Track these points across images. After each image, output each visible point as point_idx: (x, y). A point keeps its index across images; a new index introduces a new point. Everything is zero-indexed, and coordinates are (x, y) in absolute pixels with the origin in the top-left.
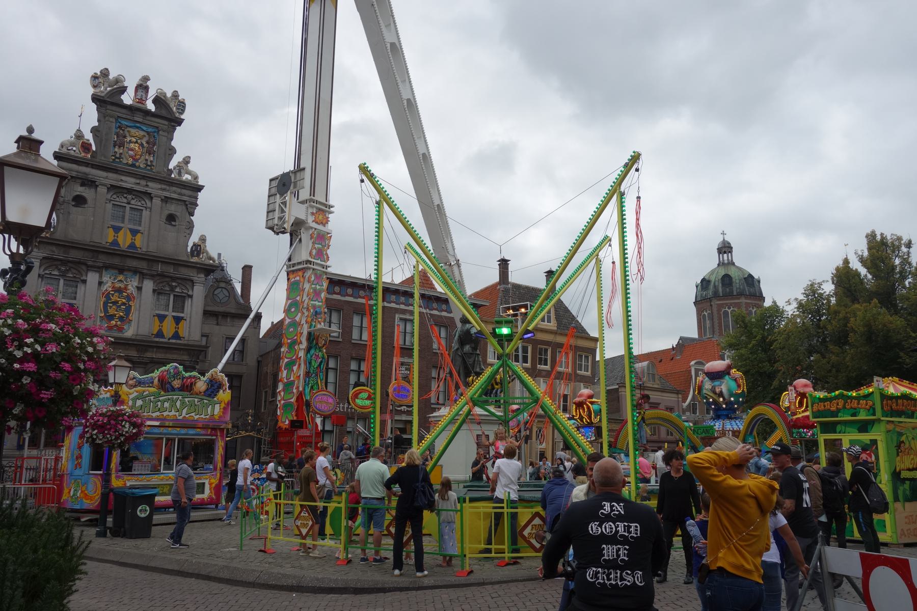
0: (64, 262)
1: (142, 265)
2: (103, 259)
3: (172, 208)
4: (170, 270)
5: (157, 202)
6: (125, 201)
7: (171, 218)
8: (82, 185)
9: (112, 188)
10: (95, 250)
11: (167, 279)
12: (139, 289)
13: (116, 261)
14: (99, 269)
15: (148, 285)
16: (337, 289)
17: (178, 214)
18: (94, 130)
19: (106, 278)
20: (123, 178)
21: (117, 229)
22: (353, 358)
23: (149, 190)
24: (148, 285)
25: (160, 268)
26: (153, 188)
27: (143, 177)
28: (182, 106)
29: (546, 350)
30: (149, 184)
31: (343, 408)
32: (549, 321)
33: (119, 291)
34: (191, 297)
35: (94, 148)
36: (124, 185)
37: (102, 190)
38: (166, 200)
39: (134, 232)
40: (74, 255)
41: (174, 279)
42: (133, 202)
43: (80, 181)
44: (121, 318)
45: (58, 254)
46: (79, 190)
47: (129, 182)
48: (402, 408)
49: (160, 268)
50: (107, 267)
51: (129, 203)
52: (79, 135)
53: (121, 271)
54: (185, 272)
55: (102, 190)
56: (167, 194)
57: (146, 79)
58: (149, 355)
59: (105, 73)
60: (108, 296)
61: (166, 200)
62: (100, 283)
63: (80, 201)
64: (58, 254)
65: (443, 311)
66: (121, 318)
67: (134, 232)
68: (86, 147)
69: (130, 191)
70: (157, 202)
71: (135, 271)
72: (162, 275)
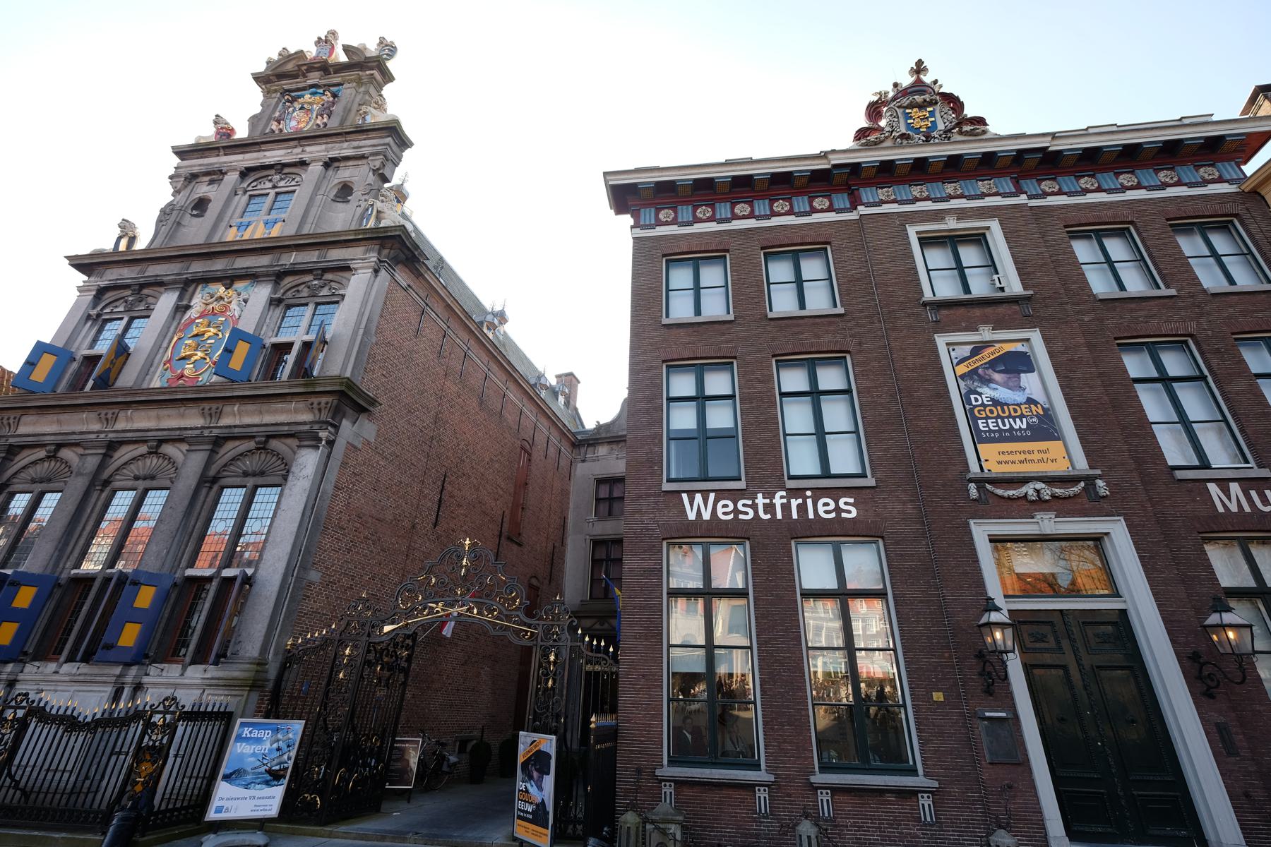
2: (198, 267)
3: (345, 174)
4: (312, 257)
5: (316, 168)
6: (269, 185)
8: (211, 182)
9: (245, 173)
11: (308, 278)
12: (246, 301)
13: (218, 265)
20: (267, 154)
23: (305, 157)
25: (291, 259)
26: (316, 151)
30: (308, 149)
31: (769, 508)
34: (343, 296)
36: (267, 161)
38: (330, 164)
42: (282, 183)
43: (207, 178)
46: (203, 189)
48: (1029, 489)
51: (274, 187)
53: (229, 280)
54: (336, 254)
69: (280, 167)
70: (316, 168)
72: (294, 272)
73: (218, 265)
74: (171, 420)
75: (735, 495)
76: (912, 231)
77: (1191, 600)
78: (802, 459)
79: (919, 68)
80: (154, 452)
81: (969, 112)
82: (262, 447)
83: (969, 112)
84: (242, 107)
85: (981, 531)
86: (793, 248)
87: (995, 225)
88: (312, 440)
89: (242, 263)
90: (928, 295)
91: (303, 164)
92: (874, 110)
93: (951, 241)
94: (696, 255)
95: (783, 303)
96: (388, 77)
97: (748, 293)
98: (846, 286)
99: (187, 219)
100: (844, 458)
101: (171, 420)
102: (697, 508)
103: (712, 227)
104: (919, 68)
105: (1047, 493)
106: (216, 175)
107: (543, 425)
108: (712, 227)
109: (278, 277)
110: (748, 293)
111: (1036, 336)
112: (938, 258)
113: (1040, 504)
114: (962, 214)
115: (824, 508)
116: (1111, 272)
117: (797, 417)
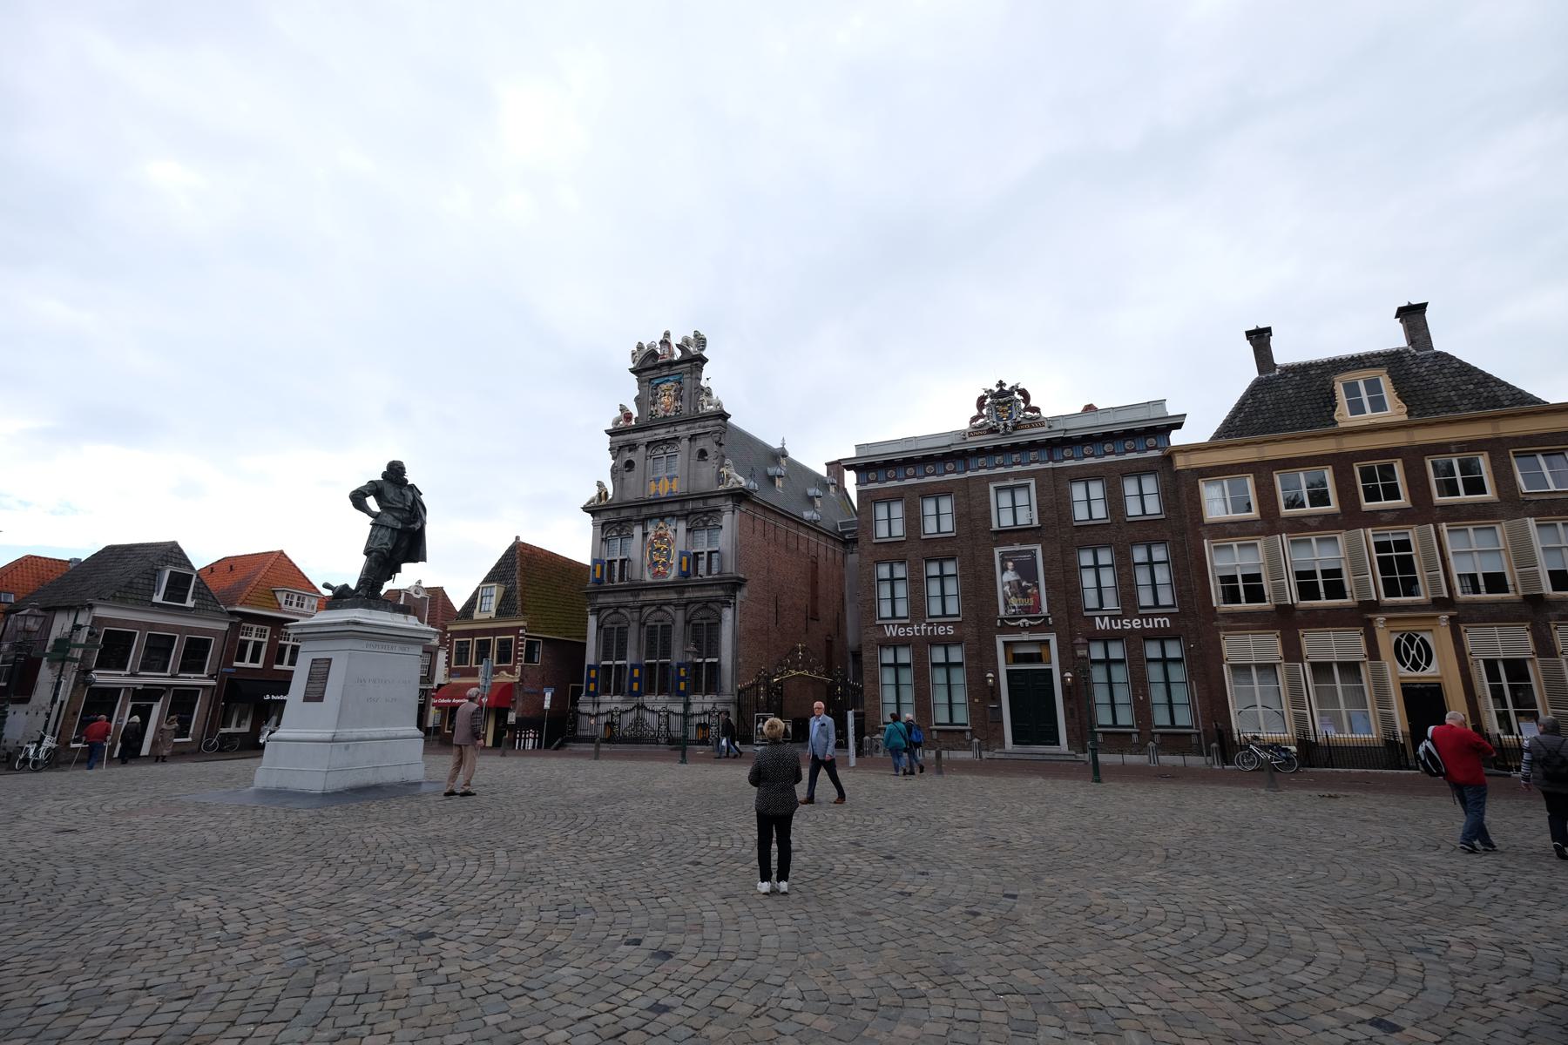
0: (620, 523)
1: (676, 507)
2: (645, 511)
4: (700, 504)
5: (685, 442)
7: (703, 454)
9: (648, 445)
10: (638, 505)
13: (655, 510)
14: (643, 522)
15: (682, 526)
16: (872, 475)
17: (706, 448)
18: (637, 399)
19: (651, 528)
21: (657, 480)
22: (928, 560)
24: (682, 526)
25: (690, 506)
26: (682, 430)
27: (672, 424)
28: (701, 341)
29: (1390, 468)
32: (1378, 404)
33: (661, 537)
35: (635, 414)
37: (642, 449)
38: (692, 438)
39: (671, 479)
40: (625, 513)
41: (706, 513)
44: (664, 564)
45: (612, 516)
46: (628, 456)
47: (661, 433)
48: (1020, 622)
49: (690, 506)
50: (650, 518)
52: (623, 408)
53: (662, 518)
54: (712, 502)
55: (642, 449)
56: (692, 432)
57: (667, 334)
58: (686, 595)
59: (640, 346)
60: (652, 542)
61: (692, 438)
62: (645, 535)
63: (630, 465)
64: (612, 516)
65: (1086, 456)
66: (664, 564)
67: (671, 479)
68: (628, 417)
69: (665, 441)
71: (672, 515)
72: (693, 512)
73: (655, 510)
74: (664, 596)
75: (905, 626)
76: (992, 487)
77: (1078, 667)
78: (935, 609)
79: (1001, 384)
80: (659, 609)
81: (1033, 403)
82: (706, 607)
83: (1033, 403)
84: (627, 391)
85: (1000, 641)
86: (936, 492)
87: (1032, 482)
88: (727, 604)
89: (667, 508)
90: (995, 526)
91: (676, 438)
92: (981, 402)
93: (1012, 489)
94: (889, 498)
95: (930, 527)
96: (704, 360)
97: (914, 520)
98: (960, 518)
99: (627, 475)
100: (953, 607)
101: (664, 596)
102: (890, 632)
103: (895, 483)
104: (1001, 384)
105: (1027, 623)
106: (632, 447)
107: (822, 541)
108: (895, 483)
109: (685, 517)
110: (914, 520)
111: (1039, 548)
112: (1005, 500)
113: (1025, 628)
114: (1017, 475)
115: (941, 630)
116: (1088, 503)
117: (934, 588)
